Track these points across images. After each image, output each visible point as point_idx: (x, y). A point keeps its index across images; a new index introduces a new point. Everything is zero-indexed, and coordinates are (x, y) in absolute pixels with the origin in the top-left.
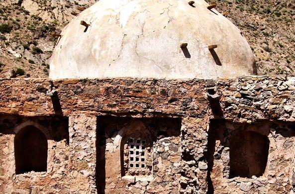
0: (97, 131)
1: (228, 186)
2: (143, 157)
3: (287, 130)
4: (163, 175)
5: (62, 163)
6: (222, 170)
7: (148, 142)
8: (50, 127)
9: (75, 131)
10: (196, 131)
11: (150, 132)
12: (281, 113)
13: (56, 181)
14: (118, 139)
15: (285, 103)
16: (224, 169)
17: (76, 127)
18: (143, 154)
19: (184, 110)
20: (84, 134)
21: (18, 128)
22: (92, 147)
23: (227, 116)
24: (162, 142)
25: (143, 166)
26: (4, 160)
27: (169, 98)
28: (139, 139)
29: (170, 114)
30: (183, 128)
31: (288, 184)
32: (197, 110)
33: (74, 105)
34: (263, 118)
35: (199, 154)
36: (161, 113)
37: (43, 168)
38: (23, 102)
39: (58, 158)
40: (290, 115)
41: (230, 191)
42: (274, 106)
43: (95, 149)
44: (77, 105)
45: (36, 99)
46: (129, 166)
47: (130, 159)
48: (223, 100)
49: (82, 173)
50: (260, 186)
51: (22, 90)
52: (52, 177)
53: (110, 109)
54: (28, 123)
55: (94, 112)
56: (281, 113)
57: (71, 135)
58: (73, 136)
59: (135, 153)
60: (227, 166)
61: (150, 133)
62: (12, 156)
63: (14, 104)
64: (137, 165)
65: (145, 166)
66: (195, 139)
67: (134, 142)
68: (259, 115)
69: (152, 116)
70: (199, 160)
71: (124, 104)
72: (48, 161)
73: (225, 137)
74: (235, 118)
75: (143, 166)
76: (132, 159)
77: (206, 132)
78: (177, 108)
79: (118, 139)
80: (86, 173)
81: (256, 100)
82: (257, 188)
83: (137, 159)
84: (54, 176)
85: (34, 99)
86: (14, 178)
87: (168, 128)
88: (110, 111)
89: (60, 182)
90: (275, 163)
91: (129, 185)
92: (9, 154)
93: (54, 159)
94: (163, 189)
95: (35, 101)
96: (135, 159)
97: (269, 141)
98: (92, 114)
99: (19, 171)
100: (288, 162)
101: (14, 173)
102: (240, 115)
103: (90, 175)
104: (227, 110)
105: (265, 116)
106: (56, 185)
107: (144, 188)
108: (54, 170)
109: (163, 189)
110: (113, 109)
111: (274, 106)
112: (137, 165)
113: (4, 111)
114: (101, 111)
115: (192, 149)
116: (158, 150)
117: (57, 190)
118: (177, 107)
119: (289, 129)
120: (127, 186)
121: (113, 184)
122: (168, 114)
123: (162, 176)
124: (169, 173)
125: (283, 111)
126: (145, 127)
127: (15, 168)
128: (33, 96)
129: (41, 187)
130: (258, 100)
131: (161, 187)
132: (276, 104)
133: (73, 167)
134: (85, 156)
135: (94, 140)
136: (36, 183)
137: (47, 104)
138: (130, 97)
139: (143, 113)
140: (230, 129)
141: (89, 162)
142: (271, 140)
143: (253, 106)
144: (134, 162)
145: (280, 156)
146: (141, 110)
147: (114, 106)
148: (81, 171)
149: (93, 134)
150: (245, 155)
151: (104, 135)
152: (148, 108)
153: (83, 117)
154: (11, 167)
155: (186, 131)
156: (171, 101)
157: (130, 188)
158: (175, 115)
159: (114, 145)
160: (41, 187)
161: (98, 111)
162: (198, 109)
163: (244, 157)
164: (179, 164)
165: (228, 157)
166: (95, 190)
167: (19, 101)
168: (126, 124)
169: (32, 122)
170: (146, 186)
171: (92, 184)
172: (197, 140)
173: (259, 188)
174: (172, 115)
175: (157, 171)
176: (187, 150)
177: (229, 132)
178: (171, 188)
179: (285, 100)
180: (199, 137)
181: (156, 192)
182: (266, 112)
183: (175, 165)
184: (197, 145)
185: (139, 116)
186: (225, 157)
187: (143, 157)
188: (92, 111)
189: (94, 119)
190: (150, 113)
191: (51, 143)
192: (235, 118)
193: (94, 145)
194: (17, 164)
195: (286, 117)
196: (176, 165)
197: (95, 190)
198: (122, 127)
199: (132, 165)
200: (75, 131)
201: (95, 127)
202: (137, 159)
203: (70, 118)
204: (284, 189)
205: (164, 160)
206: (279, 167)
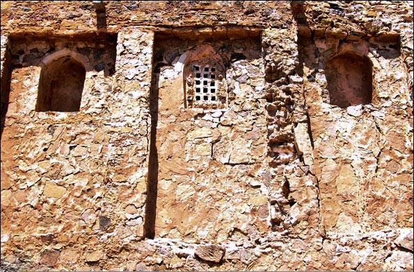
0: (154, 47)
1: (331, 112)
2: (213, 87)
3: (389, 50)
4: (243, 101)
5: (103, 94)
6: (320, 94)
7: (219, 69)
8: (91, 56)
9: (125, 47)
10: (281, 41)
11: (222, 57)
12: (379, 25)
13: (91, 116)
14: (179, 66)
15: (381, 16)
16: (323, 93)
17: (126, 43)
18: (213, 84)
19: (263, 21)
20: (136, 50)
21: (49, 59)
22: (146, 65)
23: (318, 27)
24: (237, 64)
25: (213, 99)
26: (22, 94)
27: (245, 10)
28: (207, 66)
29: (247, 26)
30: (265, 39)
31: (408, 106)
32: (279, 20)
33: (126, 20)
34: (360, 31)
35: (289, 66)
36: (235, 25)
37: (75, 106)
38: (60, 21)
39: (97, 90)
40: (390, 28)
41: (336, 117)
42: (370, 19)
43: (150, 66)
44: (130, 21)
45: (78, 17)
46: (195, 99)
47: (195, 90)
48: (310, 10)
49: (131, 95)
50: (373, 111)
51: (62, 8)
52: (86, 113)
53: (171, 23)
54: (62, 52)
55: (151, 27)
56: (379, 25)
57: (118, 52)
58: (122, 54)
59: (203, 83)
60: (326, 90)
61: (221, 59)
62: (35, 89)
63: (48, 23)
64: (206, 98)
65: (216, 98)
66: (281, 50)
67: (200, 70)
68: (355, 28)
69: (224, 29)
70: (290, 74)
71: (189, 17)
72: (83, 94)
73: (316, 57)
74: (327, 28)
75: (213, 99)
76: (198, 90)
77: (295, 42)
78: (256, 19)
79: (179, 66)
80: (137, 94)
81: (348, 12)
82: (370, 112)
83: (205, 90)
84: (90, 110)
85: (75, 16)
86: (31, 116)
87: (244, 50)
88: (172, 26)
89: (97, 118)
90: (385, 84)
91: (196, 118)
92: (30, 87)
93: (92, 90)
94: (243, 120)
95: (76, 19)
96: (202, 90)
97: (371, 64)
98: (149, 29)
99: (39, 108)
100: (401, 82)
101: (34, 109)
102: (332, 25)
103: (142, 97)
104: (316, 21)
105: (362, 29)
106: (91, 122)
107: (217, 120)
108: (90, 103)
109: (243, 120)
110: (176, 23)
111: (370, 19)
112: (206, 98)
113: (34, 31)
114: (161, 26)
115: (280, 61)
116: (234, 74)
117: (92, 128)
118: (255, 19)
119: (392, 49)
120: (193, 119)
121: (172, 117)
122: (244, 26)
123: (240, 103)
124: (250, 99)
125: (381, 23)
126: (215, 53)
127: (35, 103)
128: (74, 13)
129: (69, 126)
130: (351, 12)
131: (240, 117)
132: (372, 17)
133: (119, 88)
134: (137, 75)
135: (150, 57)
136: (63, 120)
137: (91, 20)
138: (197, 10)
139: (213, 27)
140: (321, 49)
141: (141, 81)
142: (374, 61)
143: (345, 17)
144: (202, 94)
145: (389, 75)
146: (210, 23)
147: (177, 19)
148: (130, 93)
149: (149, 50)
150: (342, 90)
151: (162, 60)
152: (220, 20)
153: (136, 32)
154: (31, 102)
155: (270, 42)
156: (247, 13)
157: (197, 122)
158: (254, 26)
159: (173, 74)
160: (69, 126)
161: (156, 26)
162: (282, 19)
163: (341, 92)
164: (263, 87)
165: (325, 80)
166: (147, 116)
167: (56, 19)
168: (190, 48)
169: (69, 51)
170: (220, 117)
171: (144, 109)
172: (284, 51)
173: (372, 114)
174: (250, 27)
175: (234, 99)
176: (273, 65)
177: (321, 51)
178: (254, 117)
179: (380, 13)
180: (287, 47)
181: (234, 123)
182: (362, 25)
183: (257, 88)
184: (285, 57)
185: (208, 30)
186: (321, 80)
187: (213, 87)
188: (149, 25)
189: (151, 34)
190: (223, 25)
191: (89, 75)
192: (327, 28)
193: (149, 62)
194: (39, 99)
195: (386, 30)
196: (259, 88)
197: (147, 116)
198: (185, 51)
199: (198, 98)
200: (125, 47)
201: (151, 43)
202: (205, 90)
203: (119, 35)
204: (405, 113)
205: (242, 85)
206: (391, 88)
